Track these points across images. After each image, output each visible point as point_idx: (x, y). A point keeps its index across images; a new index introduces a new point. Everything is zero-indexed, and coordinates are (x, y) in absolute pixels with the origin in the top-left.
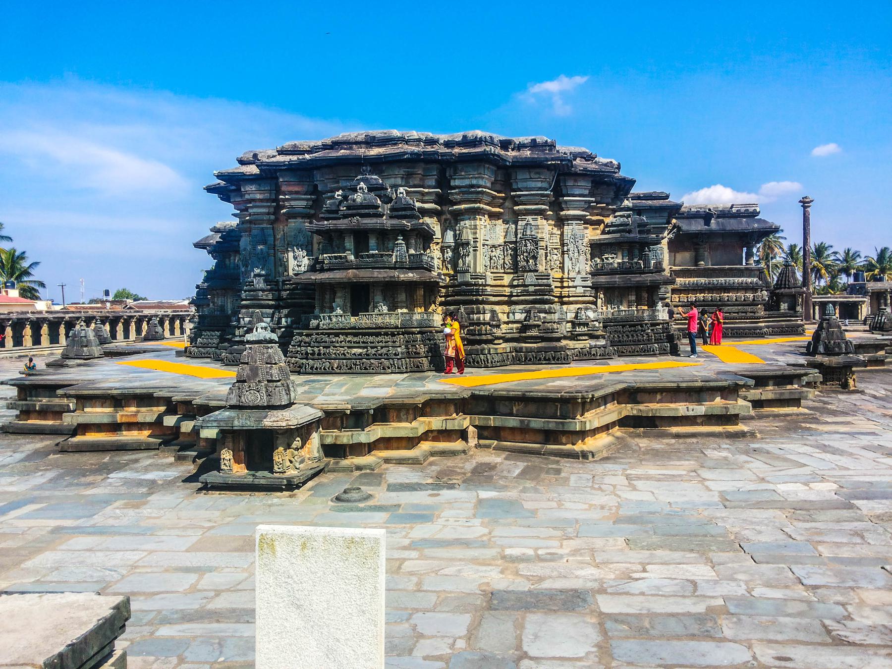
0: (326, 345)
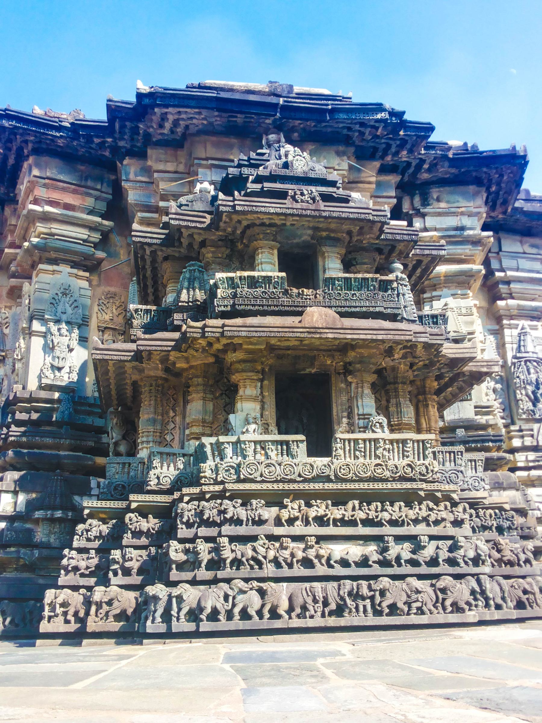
0: (242, 530)
